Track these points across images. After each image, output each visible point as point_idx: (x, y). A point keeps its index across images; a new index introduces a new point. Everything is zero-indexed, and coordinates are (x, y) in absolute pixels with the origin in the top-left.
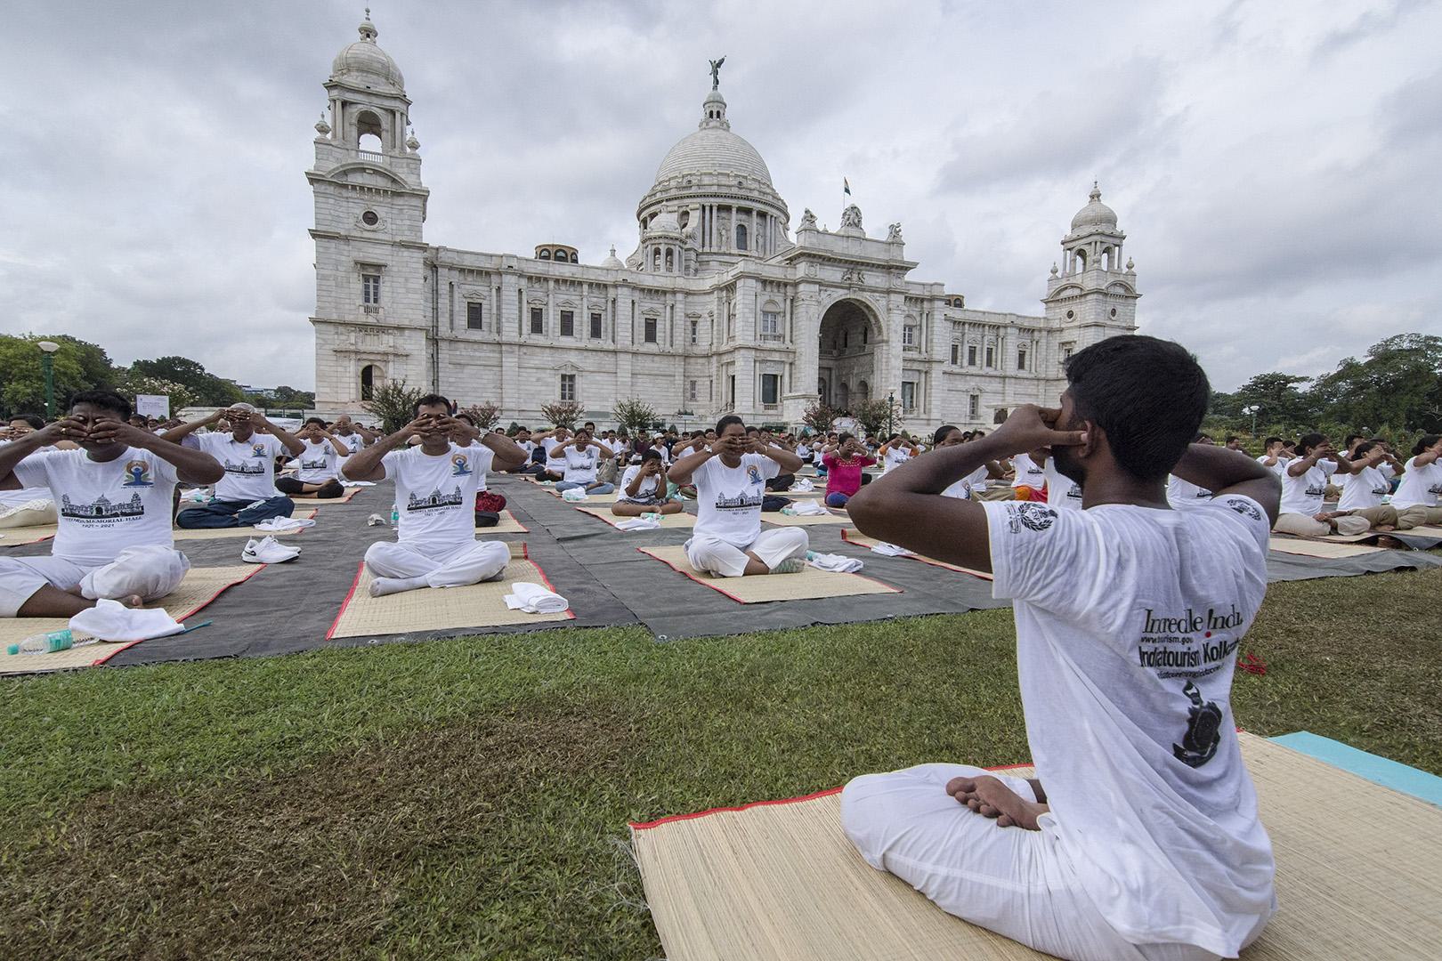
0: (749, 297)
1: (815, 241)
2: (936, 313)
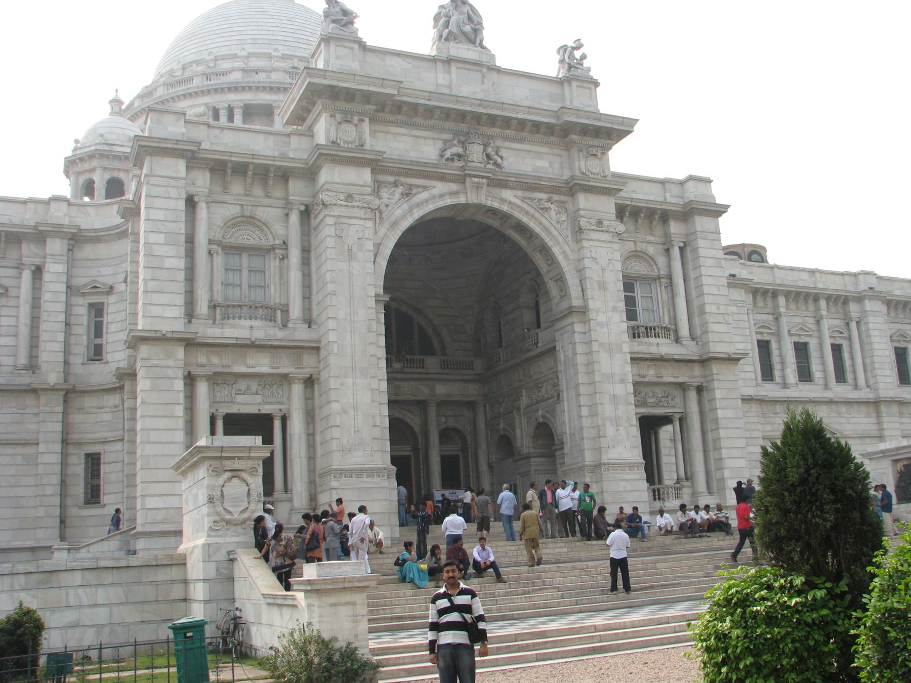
0: (171, 204)
2: (701, 243)
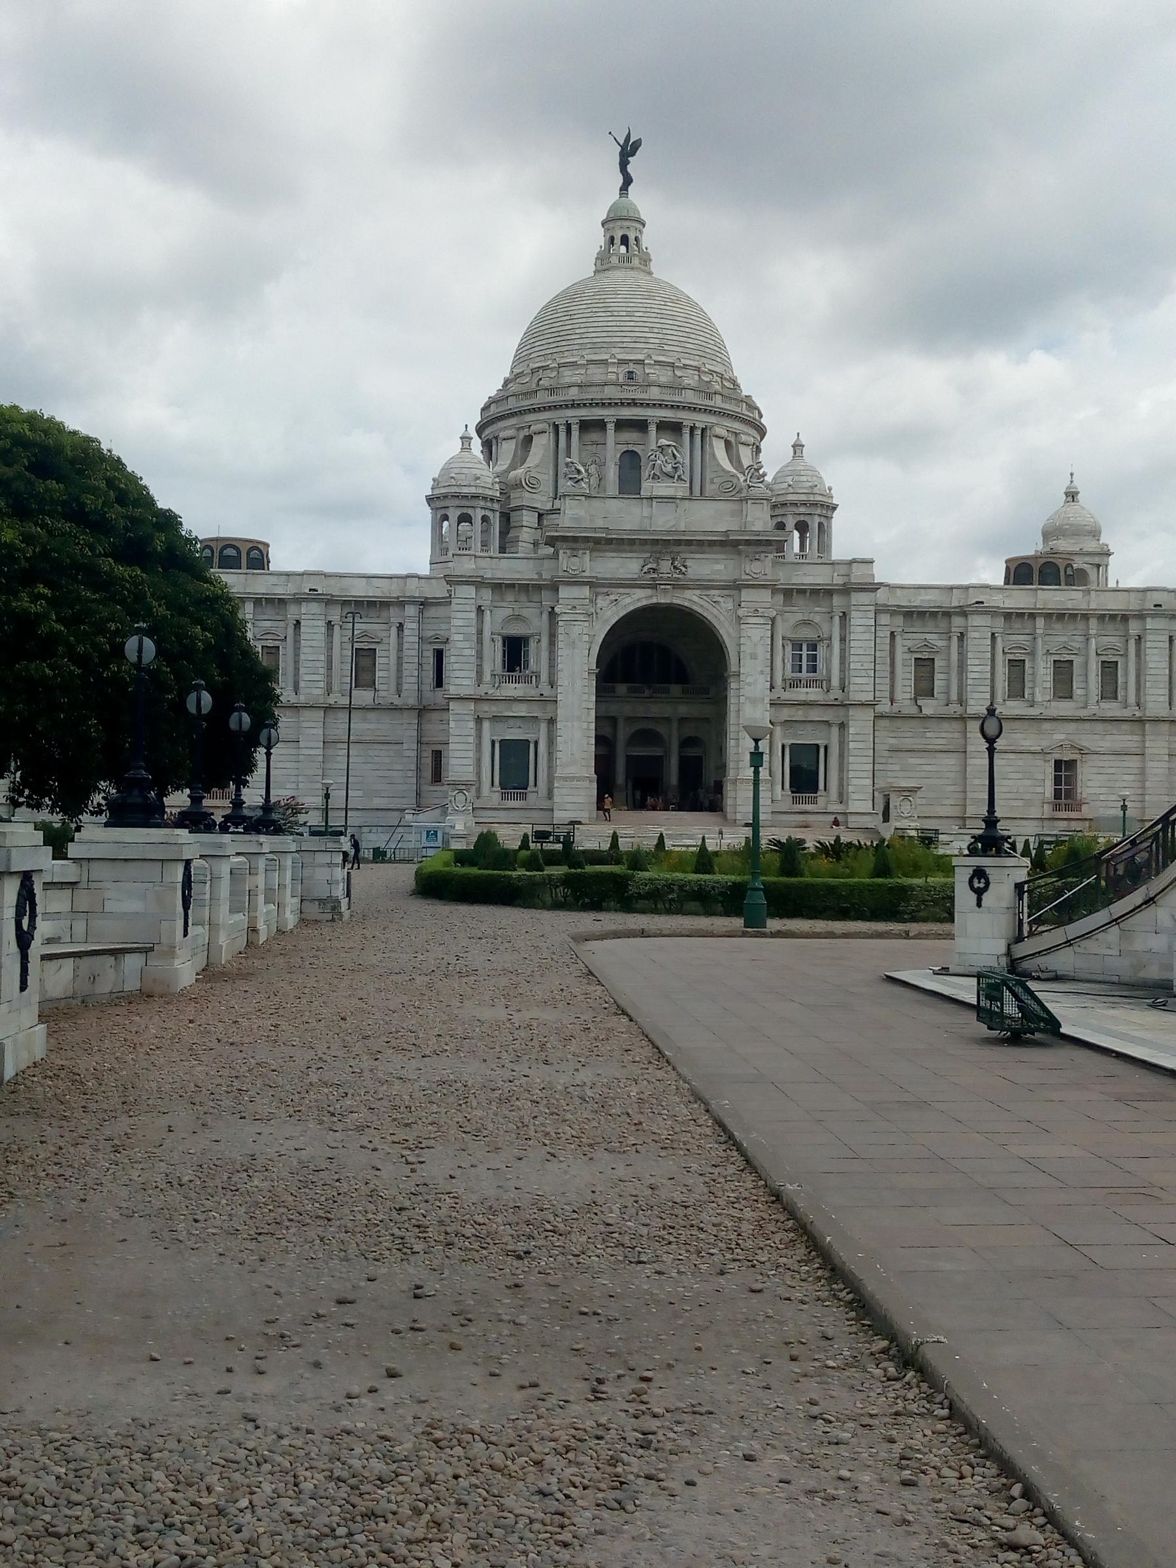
0: (465, 615)
1: (582, 513)
2: (854, 614)
